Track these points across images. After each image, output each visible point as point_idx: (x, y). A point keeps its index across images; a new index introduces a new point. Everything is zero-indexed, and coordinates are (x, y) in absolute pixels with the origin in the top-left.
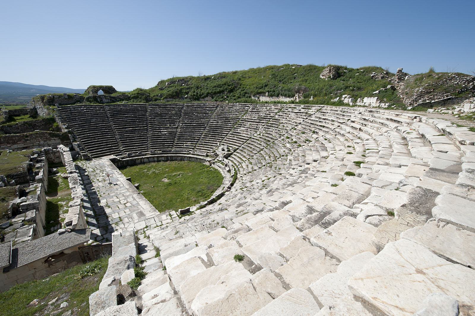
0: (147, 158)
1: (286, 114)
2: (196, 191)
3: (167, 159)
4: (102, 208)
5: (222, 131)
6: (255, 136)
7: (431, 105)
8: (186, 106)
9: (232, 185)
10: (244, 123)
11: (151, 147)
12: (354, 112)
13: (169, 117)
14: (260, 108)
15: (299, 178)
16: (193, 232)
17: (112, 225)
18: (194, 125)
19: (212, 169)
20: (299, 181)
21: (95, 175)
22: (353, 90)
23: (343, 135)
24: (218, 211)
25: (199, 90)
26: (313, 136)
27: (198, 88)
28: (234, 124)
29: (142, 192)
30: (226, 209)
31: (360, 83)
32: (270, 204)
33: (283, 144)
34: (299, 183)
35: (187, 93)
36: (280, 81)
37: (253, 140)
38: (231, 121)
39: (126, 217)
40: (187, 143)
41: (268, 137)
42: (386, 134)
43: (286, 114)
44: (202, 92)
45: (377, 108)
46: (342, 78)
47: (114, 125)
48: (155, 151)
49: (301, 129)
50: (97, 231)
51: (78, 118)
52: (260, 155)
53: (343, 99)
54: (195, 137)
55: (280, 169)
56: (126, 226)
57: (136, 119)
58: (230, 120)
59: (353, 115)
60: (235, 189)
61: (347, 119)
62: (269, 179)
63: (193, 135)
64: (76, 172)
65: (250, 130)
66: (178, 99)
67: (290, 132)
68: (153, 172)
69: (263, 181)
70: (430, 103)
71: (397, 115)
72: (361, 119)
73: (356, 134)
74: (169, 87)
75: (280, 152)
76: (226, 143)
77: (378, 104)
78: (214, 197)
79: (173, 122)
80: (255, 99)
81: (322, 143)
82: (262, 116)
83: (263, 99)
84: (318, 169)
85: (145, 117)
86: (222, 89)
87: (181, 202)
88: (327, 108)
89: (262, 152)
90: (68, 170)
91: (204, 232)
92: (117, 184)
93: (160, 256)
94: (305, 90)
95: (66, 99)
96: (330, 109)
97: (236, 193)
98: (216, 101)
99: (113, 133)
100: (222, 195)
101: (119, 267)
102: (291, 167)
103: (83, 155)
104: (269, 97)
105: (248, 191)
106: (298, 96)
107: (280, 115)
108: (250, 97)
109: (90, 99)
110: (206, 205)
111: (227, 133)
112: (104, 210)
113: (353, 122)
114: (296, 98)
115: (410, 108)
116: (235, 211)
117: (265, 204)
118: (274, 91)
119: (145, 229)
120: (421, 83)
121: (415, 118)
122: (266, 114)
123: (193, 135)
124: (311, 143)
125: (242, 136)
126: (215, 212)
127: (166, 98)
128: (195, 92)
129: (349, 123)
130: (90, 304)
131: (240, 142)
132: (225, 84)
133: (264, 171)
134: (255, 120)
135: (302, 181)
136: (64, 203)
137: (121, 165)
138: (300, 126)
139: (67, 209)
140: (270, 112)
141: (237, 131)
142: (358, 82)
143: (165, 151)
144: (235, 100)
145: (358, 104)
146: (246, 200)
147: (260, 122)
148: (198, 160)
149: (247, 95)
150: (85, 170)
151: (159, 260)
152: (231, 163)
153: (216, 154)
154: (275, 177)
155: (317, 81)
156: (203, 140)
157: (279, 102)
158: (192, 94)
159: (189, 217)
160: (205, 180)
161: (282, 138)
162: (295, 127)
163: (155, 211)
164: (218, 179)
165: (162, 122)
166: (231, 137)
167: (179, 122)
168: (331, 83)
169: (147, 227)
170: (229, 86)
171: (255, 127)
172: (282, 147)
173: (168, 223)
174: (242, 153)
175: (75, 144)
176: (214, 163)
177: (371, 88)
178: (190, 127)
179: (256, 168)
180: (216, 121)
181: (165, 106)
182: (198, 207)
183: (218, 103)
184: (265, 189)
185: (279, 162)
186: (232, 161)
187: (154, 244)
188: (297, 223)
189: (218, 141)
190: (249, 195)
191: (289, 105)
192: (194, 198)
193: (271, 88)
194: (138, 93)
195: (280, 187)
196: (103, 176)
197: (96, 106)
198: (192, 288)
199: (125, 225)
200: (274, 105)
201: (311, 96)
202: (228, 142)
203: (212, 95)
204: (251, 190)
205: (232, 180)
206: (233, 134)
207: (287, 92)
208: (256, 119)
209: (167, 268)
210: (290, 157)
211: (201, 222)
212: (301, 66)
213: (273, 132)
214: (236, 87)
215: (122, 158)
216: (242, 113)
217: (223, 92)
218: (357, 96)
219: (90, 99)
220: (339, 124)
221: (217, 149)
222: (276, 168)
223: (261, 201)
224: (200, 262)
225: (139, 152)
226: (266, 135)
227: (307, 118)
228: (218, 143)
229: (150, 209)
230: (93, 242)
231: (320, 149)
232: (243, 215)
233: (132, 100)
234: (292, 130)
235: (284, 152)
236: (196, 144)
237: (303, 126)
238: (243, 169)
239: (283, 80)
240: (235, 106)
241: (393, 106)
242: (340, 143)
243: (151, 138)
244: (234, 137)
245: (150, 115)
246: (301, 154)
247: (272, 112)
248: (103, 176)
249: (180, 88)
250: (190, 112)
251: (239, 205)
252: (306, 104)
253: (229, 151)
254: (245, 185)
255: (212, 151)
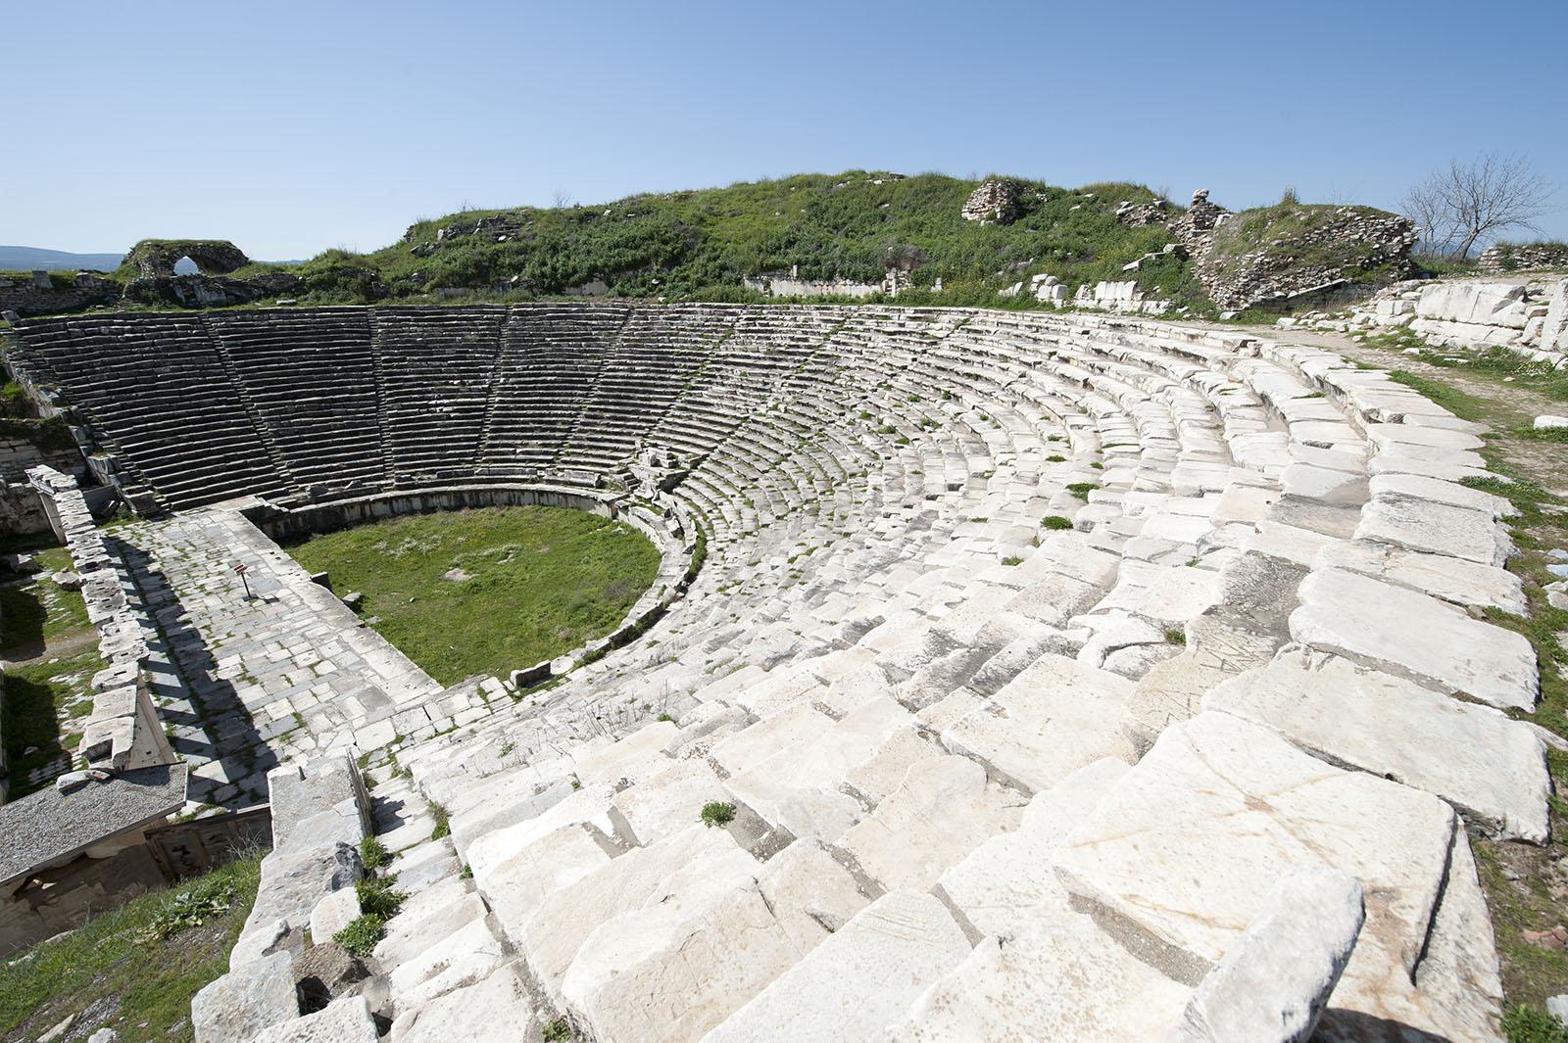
0: (385, 500)
1: (858, 337)
2: (570, 605)
3: (459, 502)
4: (225, 686)
5: (649, 399)
6: (760, 415)
7: (1286, 307)
8: (515, 313)
9: (691, 578)
10: (720, 369)
11: (397, 460)
12: (1066, 328)
13: (458, 352)
14: (773, 319)
15: (903, 546)
16: (564, 744)
17: (269, 744)
18: (550, 382)
19: (619, 528)
20: (904, 554)
21: (188, 572)
22: (1064, 259)
23: (1037, 404)
24: (648, 667)
25: (561, 257)
26: (944, 408)
27: (555, 249)
28: (687, 374)
29: (373, 620)
30: (675, 660)
31: (1085, 235)
32: (815, 633)
33: (851, 438)
34: (903, 559)
35: (518, 268)
36: (835, 228)
37: (753, 426)
38: (676, 364)
39: (319, 712)
40: (526, 445)
41: (804, 415)
42: (1161, 395)
43: (858, 337)
44: (571, 263)
45: (1136, 317)
46: (1031, 219)
47: (248, 385)
48: (414, 474)
49: (908, 386)
50: (213, 770)
51: (104, 364)
52: (780, 477)
53: (1033, 287)
54: (554, 422)
55: (843, 518)
56: (322, 743)
57: (334, 364)
58: (674, 360)
59: (1063, 340)
60: (701, 593)
61: (1047, 351)
62: (810, 552)
63: (549, 415)
64: (111, 565)
65: (744, 395)
66: (484, 291)
67: (872, 398)
68: (408, 549)
69: (791, 561)
70: (1284, 298)
71: (1193, 337)
72: (1087, 351)
73: (1076, 398)
74: (448, 247)
75: (842, 463)
76: (663, 439)
77: (1139, 304)
78: (633, 623)
79: (473, 372)
80: (756, 290)
81: (973, 430)
82: (779, 345)
83: (782, 288)
84: (962, 513)
85: (368, 356)
86: (640, 253)
87: (518, 645)
88: (986, 318)
89: (784, 466)
90: (77, 558)
91: (600, 739)
92: (276, 600)
93: (449, 833)
94: (916, 260)
95: (45, 291)
96: (995, 320)
97: (706, 603)
98: (622, 294)
99: (248, 416)
100: (659, 613)
101: (299, 885)
102: (878, 510)
103: (132, 500)
104: (803, 283)
105: (744, 594)
106: (897, 277)
107: (838, 343)
108: (738, 282)
109: (144, 292)
110: (606, 649)
111: (667, 404)
112: (234, 694)
113: (1066, 360)
114: (888, 286)
115: (1228, 315)
116: (703, 662)
117: (798, 633)
118: (817, 263)
119: (395, 748)
120: (1260, 237)
121: (1244, 344)
122: (792, 339)
123: (549, 415)
124: (939, 430)
125: (718, 414)
126: (637, 671)
127: (440, 285)
128: (544, 264)
129: (1053, 363)
130: (197, 1025)
131: (710, 435)
132: (651, 237)
133: (793, 527)
134: (759, 358)
135: (915, 554)
136: (72, 680)
137: (286, 531)
138: (903, 377)
139: (87, 698)
140: (806, 333)
141: (698, 399)
142: (1079, 234)
143: (449, 475)
144: (687, 290)
145: (1079, 302)
146: (739, 626)
147: (774, 367)
148: (571, 502)
149: (727, 275)
150: (146, 554)
151: (447, 846)
152: (683, 508)
153: (633, 476)
154: (829, 544)
155: (954, 229)
156: (586, 431)
157: (834, 300)
158: (538, 272)
159: (550, 693)
160: (599, 568)
161: (849, 416)
162: (890, 382)
163: (426, 682)
164: (644, 561)
165: (431, 372)
166: (679, 417)
167: (494, 370)
168: (996, 235)
169: (399, 739)
170: (665, 242)
171: (758, 382)
172: (850, 448)
173: (476, 721)
174: (721, 472)
175: (98, 461)
176: (626, 508)
177: (1116, 252)
178: (534, 388)
179: (766, 518)
180: (626, 364)
181: (439, 317)
182: (578, 657)
183: (629, 301)
184: (797, 585)
185: (840, 496)
186: (686, 499)
187: (428, 794)
188: (899, 685)
189: (638, 435)
190: (747, 609)
191: (869, 309)
192: (562, 629)
193: (807, 253)
194: (333, 269)
195: (847, 576)
196: (220, 573)
197: (172, 316)
198: (563, 926)
199: (317, 741)
200: (817, 309)
201: (936, 276)
202: (671, 436)
203: (608, 274)
204: (752, 591)
205: (690, 562)
206: (686, 409)
207: (859, 266)
208: (762, 355)
209: (474, 871)
210: (874, 479)
211: (589, 708)
212: (902, 177)
213: (819, 397)
214: (689, 247)
215: (291, 506)
216: (713, 337)
217: (643, 263)
218: (1075, 278)
219: (144, 292)
220: (1023, 369)
221: (633, 462)
222: (832, 514)
223: (787, 625)
224: (587, 839)
225: (352, 481)
226: (797, 409)
227: (924, 352)
228: (638, 441)
229: (406, 677)
230: (202, 810)
231: (966, 449)
232: (730, 673)
233: (312, 293)
234: (880, 389)
235: (856, 462)
236: (561, 445)
237: (912, 376)
238: (725, 525)
239: (844, 224)
240: (689, 313)
241: (1180, 310)
242: (1026, 430)
243: (393, 430)
244: (690, 418)
245: (386, 348)
246: (908, 469)
247: (814, 333)
248: (220, 573)
249: (489, 249)
250: (531, 336)
251: (718, 643)
252: (920, 304)
253: (675, 465)
254: (734, 575)
255: (616, 469)
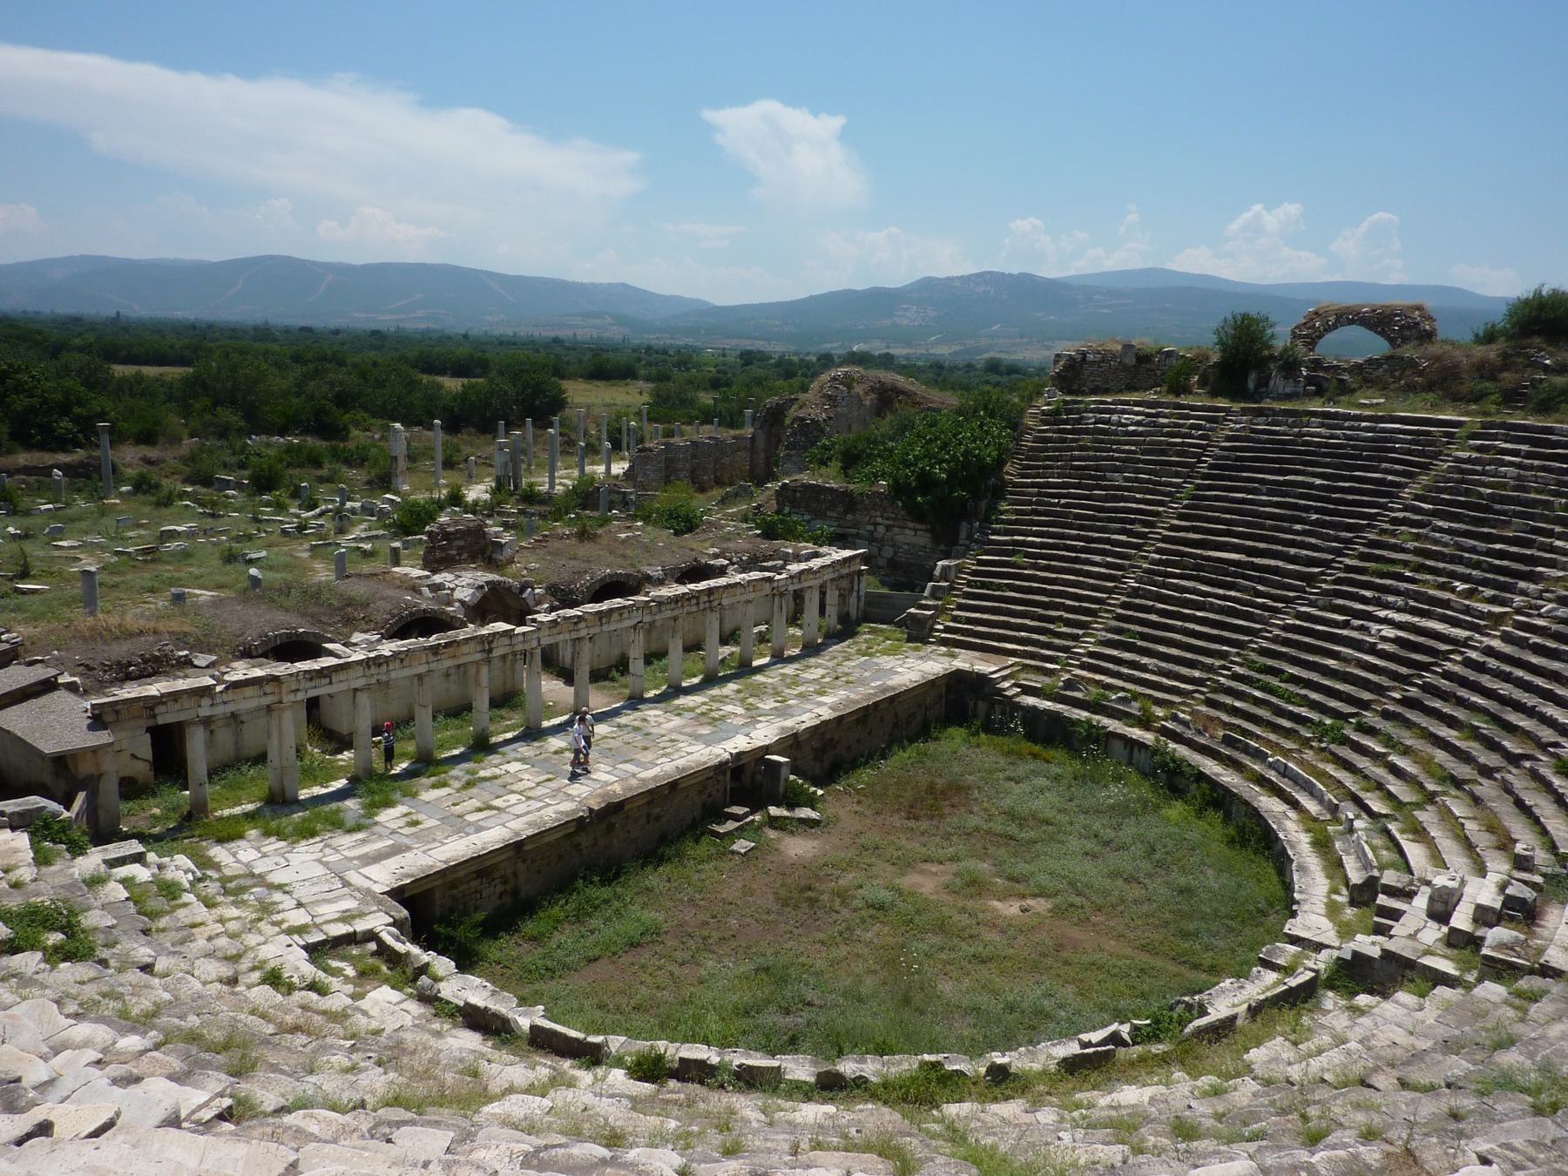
215: (1028, 691)
